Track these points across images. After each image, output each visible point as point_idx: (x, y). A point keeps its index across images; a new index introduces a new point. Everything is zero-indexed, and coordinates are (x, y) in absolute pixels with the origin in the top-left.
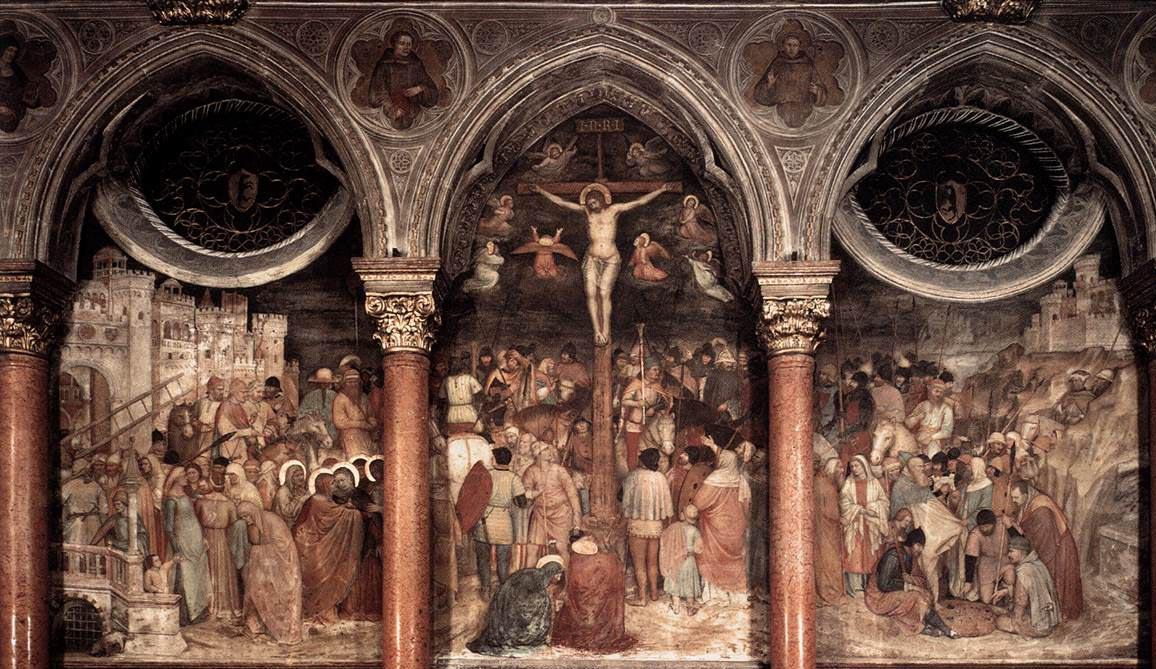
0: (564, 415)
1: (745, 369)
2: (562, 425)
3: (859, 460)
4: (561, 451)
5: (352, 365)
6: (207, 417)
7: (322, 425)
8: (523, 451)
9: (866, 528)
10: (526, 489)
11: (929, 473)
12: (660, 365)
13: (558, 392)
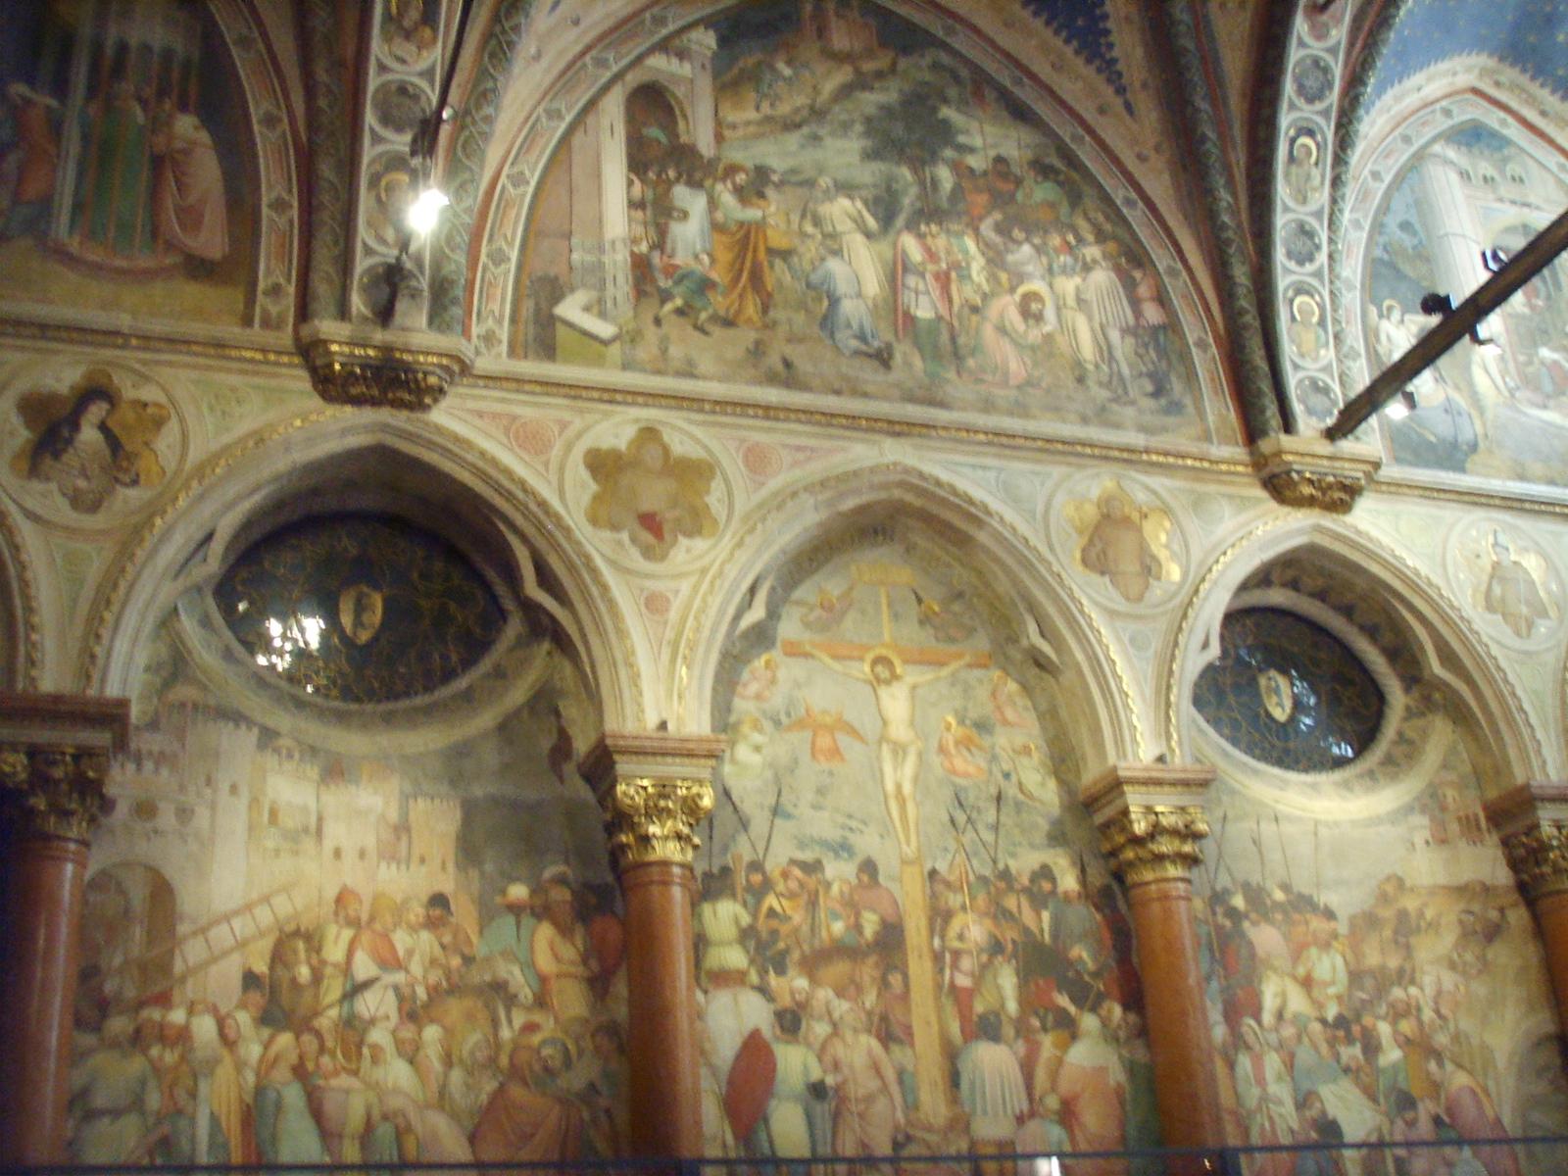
0: (872, 960)
2: (868, 971)
3: (1250, 1026)
4: (869, 1014)
5: (561, 880)
6: (335, 952)
7: (516, 971)
9: (1271, 1119)
10: (825, 1072)
11: (1332, 1043)
12: (989, 893)
13: (858, 928)
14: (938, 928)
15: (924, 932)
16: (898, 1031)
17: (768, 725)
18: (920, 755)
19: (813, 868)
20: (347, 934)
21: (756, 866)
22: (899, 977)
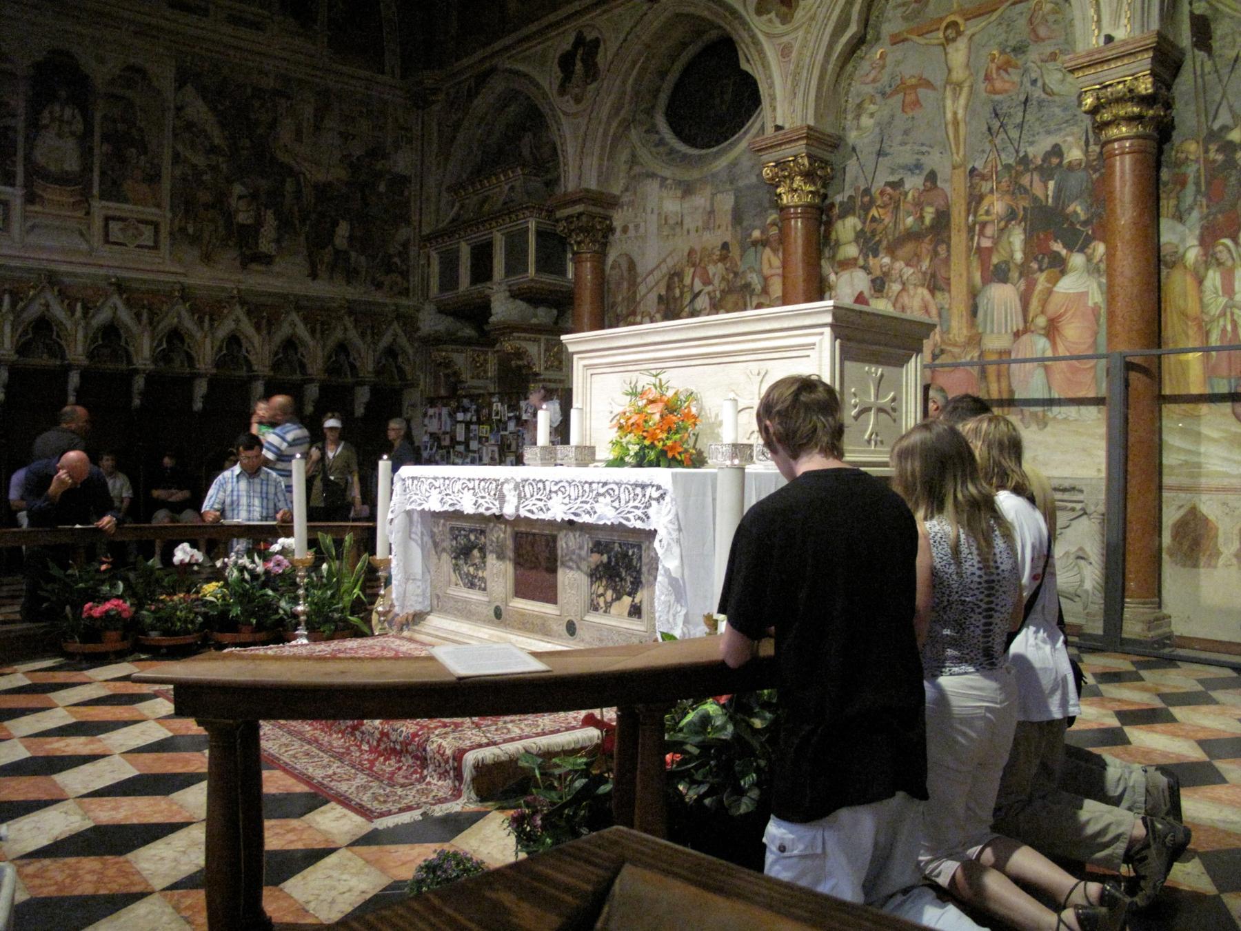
1: (1095, 163)
2: (926, 246)
6: (687, 281)
7: (754, 276)
8: (894, 278)
12: (1010, 176)
13: (922, 218)
14: (972, 210)
15: (963, 214)
16: (941, 283)
17: (878, 98)
18: (971, 86)
19: (900, 183)
20: (692, 270)
21: (867, 192)
22: (944, 246)
